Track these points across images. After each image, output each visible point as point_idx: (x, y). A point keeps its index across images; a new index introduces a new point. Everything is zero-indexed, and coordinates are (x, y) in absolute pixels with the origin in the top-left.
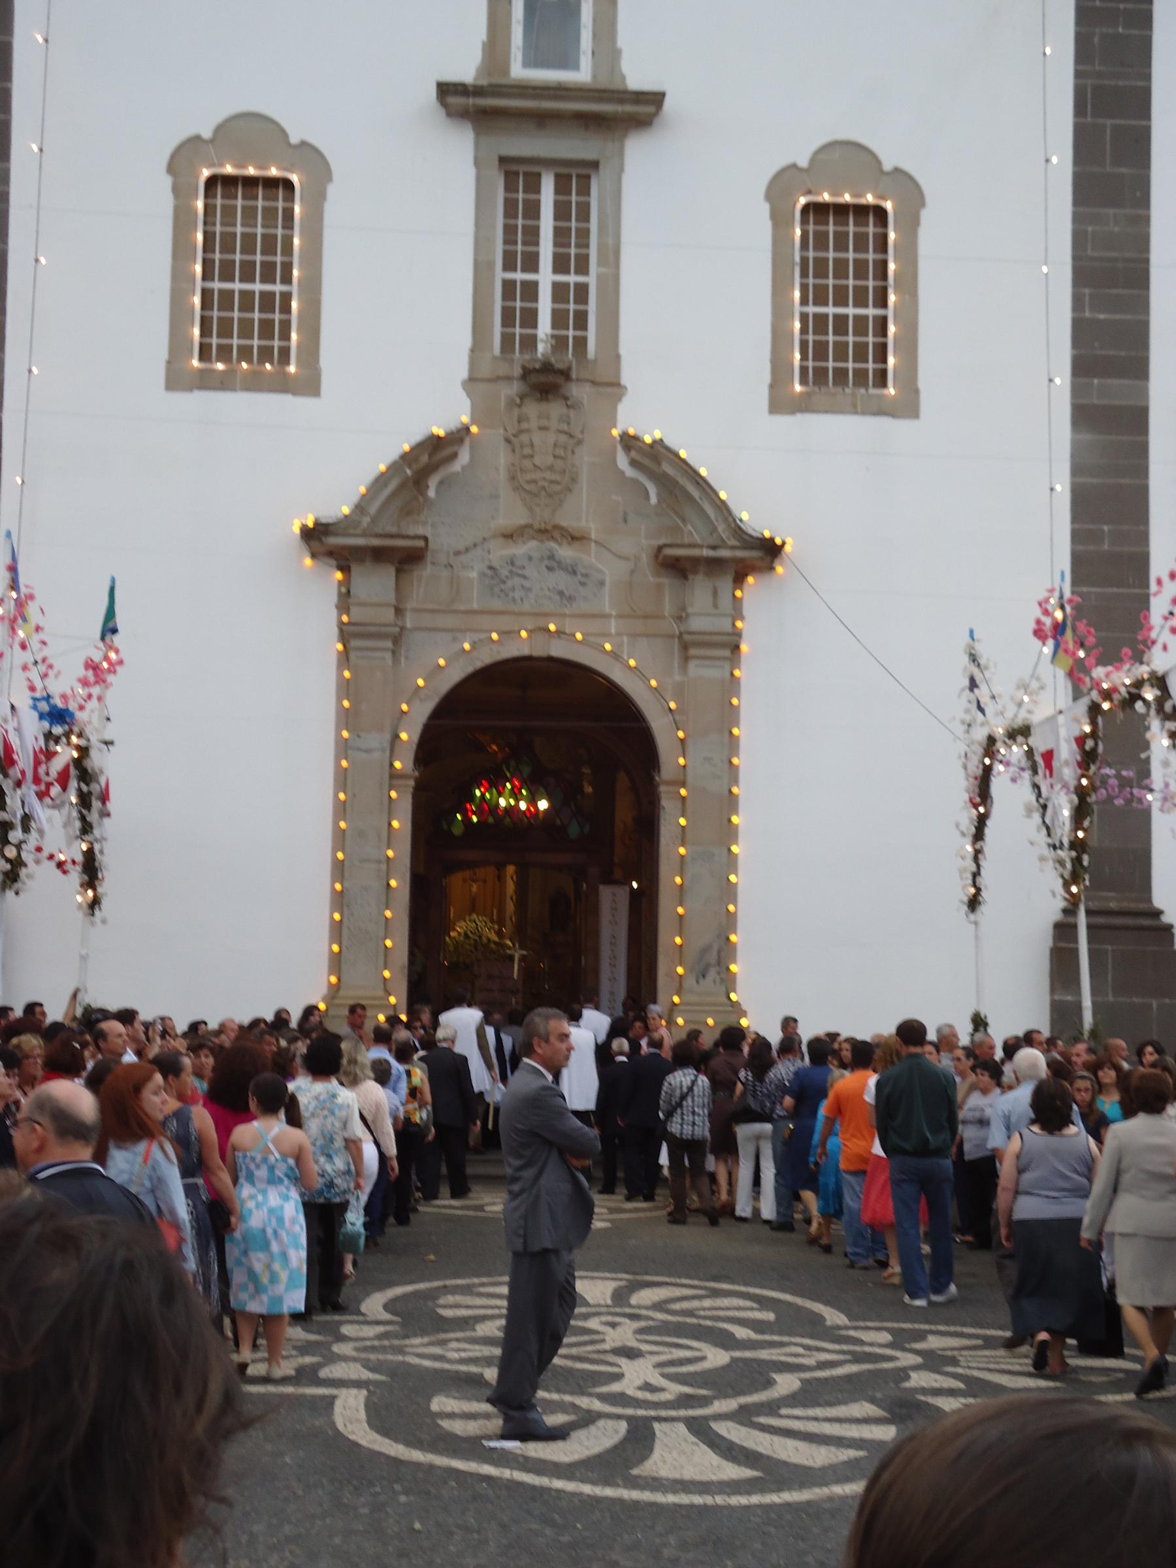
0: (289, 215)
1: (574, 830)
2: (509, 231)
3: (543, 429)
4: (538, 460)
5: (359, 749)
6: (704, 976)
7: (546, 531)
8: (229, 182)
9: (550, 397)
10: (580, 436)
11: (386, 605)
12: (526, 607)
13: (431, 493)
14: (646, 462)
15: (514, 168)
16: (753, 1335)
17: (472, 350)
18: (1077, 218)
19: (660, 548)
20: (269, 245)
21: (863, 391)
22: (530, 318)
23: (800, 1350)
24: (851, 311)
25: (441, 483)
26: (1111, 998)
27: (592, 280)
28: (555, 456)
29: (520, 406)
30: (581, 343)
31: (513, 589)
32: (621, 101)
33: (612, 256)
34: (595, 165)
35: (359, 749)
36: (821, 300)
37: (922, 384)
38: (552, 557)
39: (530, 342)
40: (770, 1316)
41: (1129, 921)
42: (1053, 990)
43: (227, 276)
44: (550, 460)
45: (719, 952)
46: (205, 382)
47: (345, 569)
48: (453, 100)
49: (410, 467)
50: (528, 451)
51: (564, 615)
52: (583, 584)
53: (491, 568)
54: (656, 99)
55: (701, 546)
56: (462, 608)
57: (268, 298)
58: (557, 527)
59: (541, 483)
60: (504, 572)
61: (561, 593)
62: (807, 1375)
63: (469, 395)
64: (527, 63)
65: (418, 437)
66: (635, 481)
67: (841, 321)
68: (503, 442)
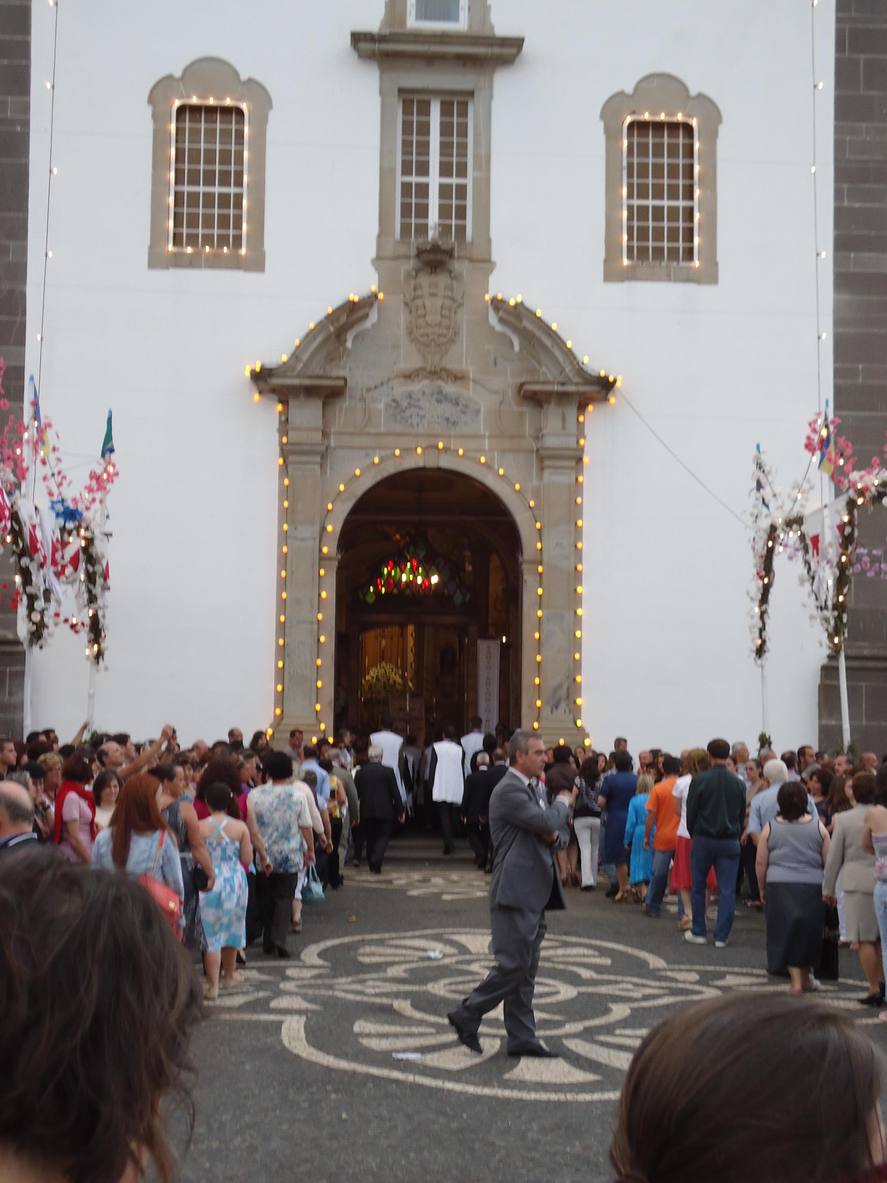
0: (240, 135)
1: (458, 599)
2: (407, 146)
3: (433, 295)
4: (429, 318)
5: (296, 538)
6: (557, 708)
8: (195, 110)
9: (438, 270)
10: (461, 301)
11: (316, 429)
12: (421, 430)
13: (349, 344)
14: (512, 319)
15: (410, 97)
16: (594, 976)
17: (379, 236)
18: (838, 130)
19: (522, 385)
20: (225, 157)
21: (675, 264)
22: (423, 211)
23: (630, 986)
24: (666, 203)
25: (356, 337)
26: (864, 722)
27: (469, 181)
28: (442, 316)
29: (415, 277)
30: (461, 229)
31: (411, 416)
32: (491, 45)
33: (484, 163)
34: (471, 94)
35: (296, 538)
36: (643, 195)
37: (720, 258)
38: (440, 392)
39: (422, 229)
40: (608, 961)
42: (820, 717)
43: (194, 181)
44: (438, 319)
45: (568, 688)
46: (178, 262)
47: (284, 402)
48: (364, 46)
49: (333, 324)
50: (421, 312)
51: (449, 436)
52: (464, 412)
53: (394, 400)
54: (517, 43)
55: (553, 383)
56: (373, 431)
57: (224, 200)
58: (444, 370)
59: (431, 337)
60: (404, 404)
61: (447, 420)
62: (636, 1005)
63: (376, 269)
64: (419, 17)
65: (338, 302)
66: (503, 335)
67: (658, 212)
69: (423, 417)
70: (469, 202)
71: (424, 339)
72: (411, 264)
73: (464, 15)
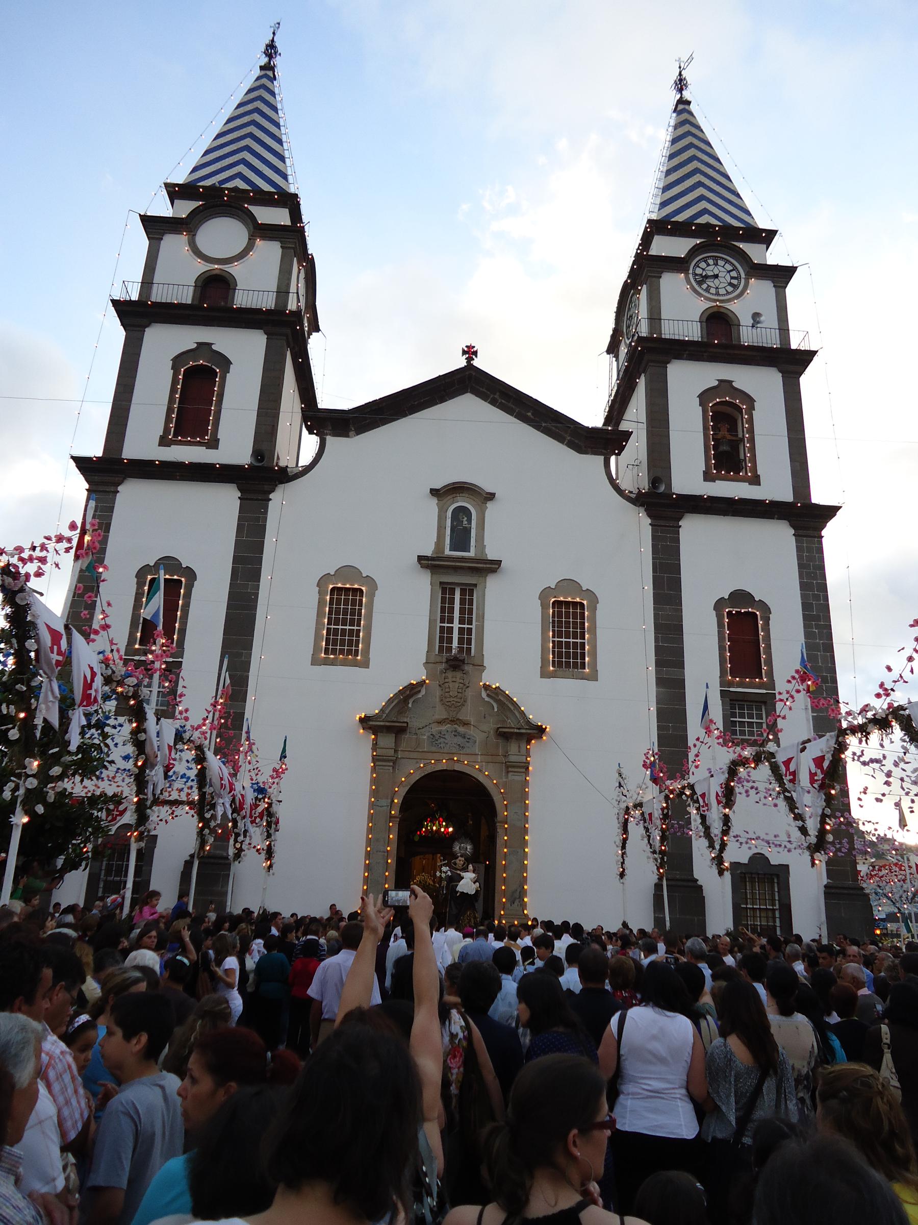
0: (361, 601)
2: (443, 610)
4: (451, 694)
7: (454, 721)
12: (445, 751)
13: (410, 705)
14: (493, 695)
18: (655, 609)
19: (498, 728)
21: (576, 670)
22: (450, 640)
27: (473, 627)
30: (469, 650)
31: (440, 744)
32: (486, 563)
33: (481, 618)
34: (475, 585)
37: (599, 668)
41: (685, 884)
43: (336, 624)
44: (456, 694)
45: (520, 892)
46: (326, 662)
48: (422, 562)
49: (402, 696)
52: (467, 742)
54: (499, 563)
55: (514, 728)
57: (351, 631)
58: (458, 719)
59: (453, 702)
60: (437, 737)
64: (450, 550)
67: (568, 643)
69: (447, 744)
70: (473, 637)
71: (447, 704)
73: (472, 549)
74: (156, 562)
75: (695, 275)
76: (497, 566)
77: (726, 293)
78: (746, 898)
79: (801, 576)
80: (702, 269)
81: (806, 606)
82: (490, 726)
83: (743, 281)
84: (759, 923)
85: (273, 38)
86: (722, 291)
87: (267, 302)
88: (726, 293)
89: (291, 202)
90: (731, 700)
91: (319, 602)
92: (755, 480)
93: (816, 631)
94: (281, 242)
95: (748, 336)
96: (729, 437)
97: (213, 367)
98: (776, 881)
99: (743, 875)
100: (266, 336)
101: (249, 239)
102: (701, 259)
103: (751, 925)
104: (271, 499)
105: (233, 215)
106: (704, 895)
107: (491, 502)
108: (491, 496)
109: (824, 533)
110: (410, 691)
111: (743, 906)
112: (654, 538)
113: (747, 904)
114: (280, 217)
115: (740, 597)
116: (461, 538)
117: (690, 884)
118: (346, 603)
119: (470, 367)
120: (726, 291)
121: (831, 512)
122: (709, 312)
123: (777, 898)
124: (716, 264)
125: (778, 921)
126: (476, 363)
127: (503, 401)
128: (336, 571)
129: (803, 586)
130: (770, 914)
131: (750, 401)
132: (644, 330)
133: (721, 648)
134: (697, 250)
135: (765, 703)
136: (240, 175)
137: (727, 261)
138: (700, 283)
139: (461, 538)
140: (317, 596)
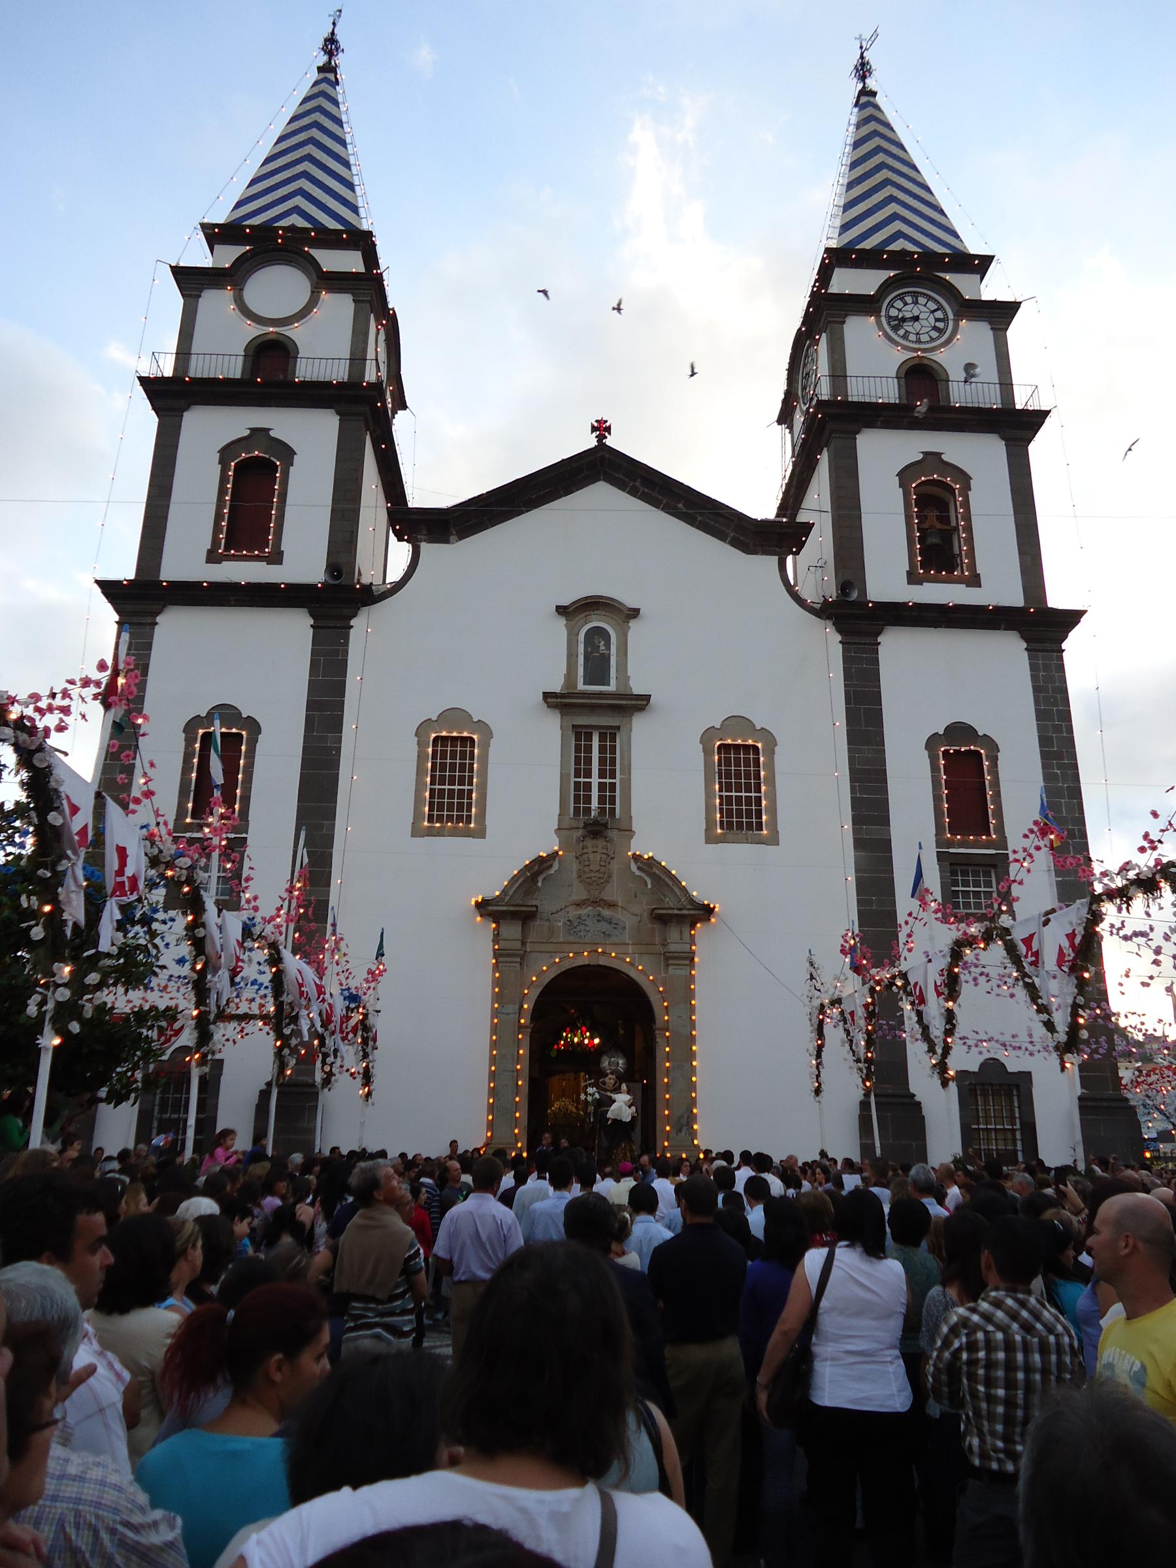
0: (472, 753)
2: (577, 760)
6: (680, 1131)
7: (596, 902)
12: (586, 940)
13: (540, 884)
14: (645, 868)
15: (580, 730)
17: (560, 815)
18: (849, 749)
22: (588, 799)
25: (544, 879)
26: (891, 1141)
27: (617, 781)
28: (601, 866)
30: (613, 811)
31: (580, 931)
32: (631, 699)
33: (627, 770)
34: (618, 728)
36: (729, 790)
38: (599, 915)
39: (588, 811)
46: (430, 832)
48: (549, 700)
49: (529, 871)
50: (587, 863)
51: (605, 944)
52: (615, 928)
55: (673, 909)
57: (461, 792)
58: (602, 900)
61: (604, 932)
64: (584, 684)
67: (739, 798)
68: (575, 859)
69: (589, 931)
70: (618, 793)
72: (580, 833)
73: (613, 681)
74: (208, 713)
75: (889, 318)
76: (645, 703)
77: (929, 339)
78: (978, 1117)
79: (1037, 702)
80: (898, 309)
81: (1044, 741)
82: (642, 907)
83: (951, 323)
84: (994, 1148)
85: (333, 30)
86: (924, 338)
87: (339, 373)
88: (929, 339)
89: (364, 242)
90: (951, 864)
91: (419, 756)
92: (974, 581)
93: (1059, 772)
94: (353, 295)
95: (960, 395)
96: (939, 526)
97: (272, 458)
98: (1015, 1093)
99: (973, 1087)
100: (338, 417)
101: (313, 292)
102: (896, 296)
103: (984, 1149)
104: (352, 627)
105: (290, 262)
106: (923, 1114)
107: (636, 620)
108: (635, 613)
109: (1064, 645)
110: (539, 866)
111: (973, 1127)
112: (846, 659)
113: (978, 1124)
114: (350, 262)
115: (959, 731)
116: (597, 668)
117: (906, 1100)
118: (453, 756)
119: (601, 447)
120: (930, 337)
121: (1072, 618)
122: (906, 367)
123: (1017, 1115)
124: (916, 303)
125: (1019, 1143)
126: (610, 441)
127: (646, 490)
128: (439, 716)
129: (1041, 715)
130: (1009, 1136)
131: (964, 478)
132: (825, 391)
133: (937, 799)
134: (889, 286)
135: (995, 866)
136: (297, 210)
137: (930, 298)
138: (895, 329)
139: (597, 668)
140: (416, 748)
